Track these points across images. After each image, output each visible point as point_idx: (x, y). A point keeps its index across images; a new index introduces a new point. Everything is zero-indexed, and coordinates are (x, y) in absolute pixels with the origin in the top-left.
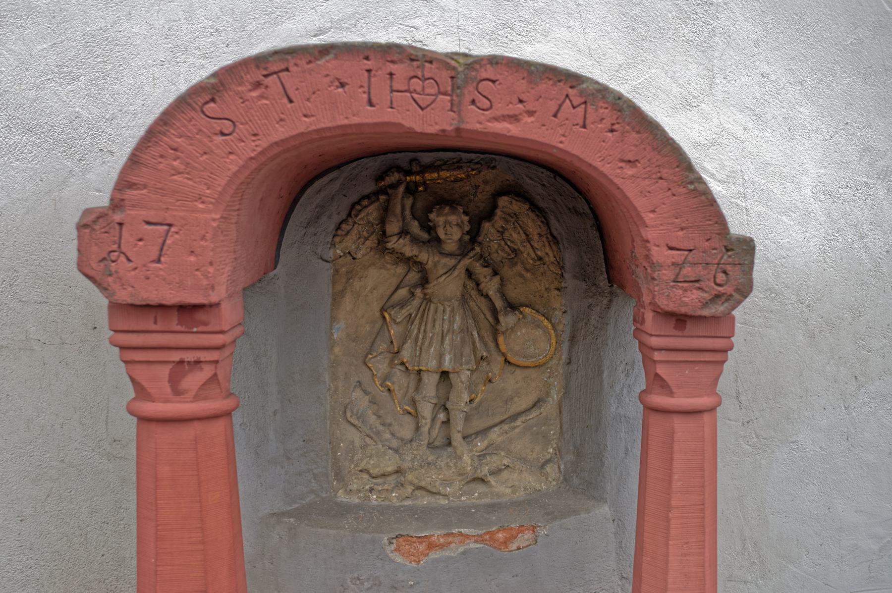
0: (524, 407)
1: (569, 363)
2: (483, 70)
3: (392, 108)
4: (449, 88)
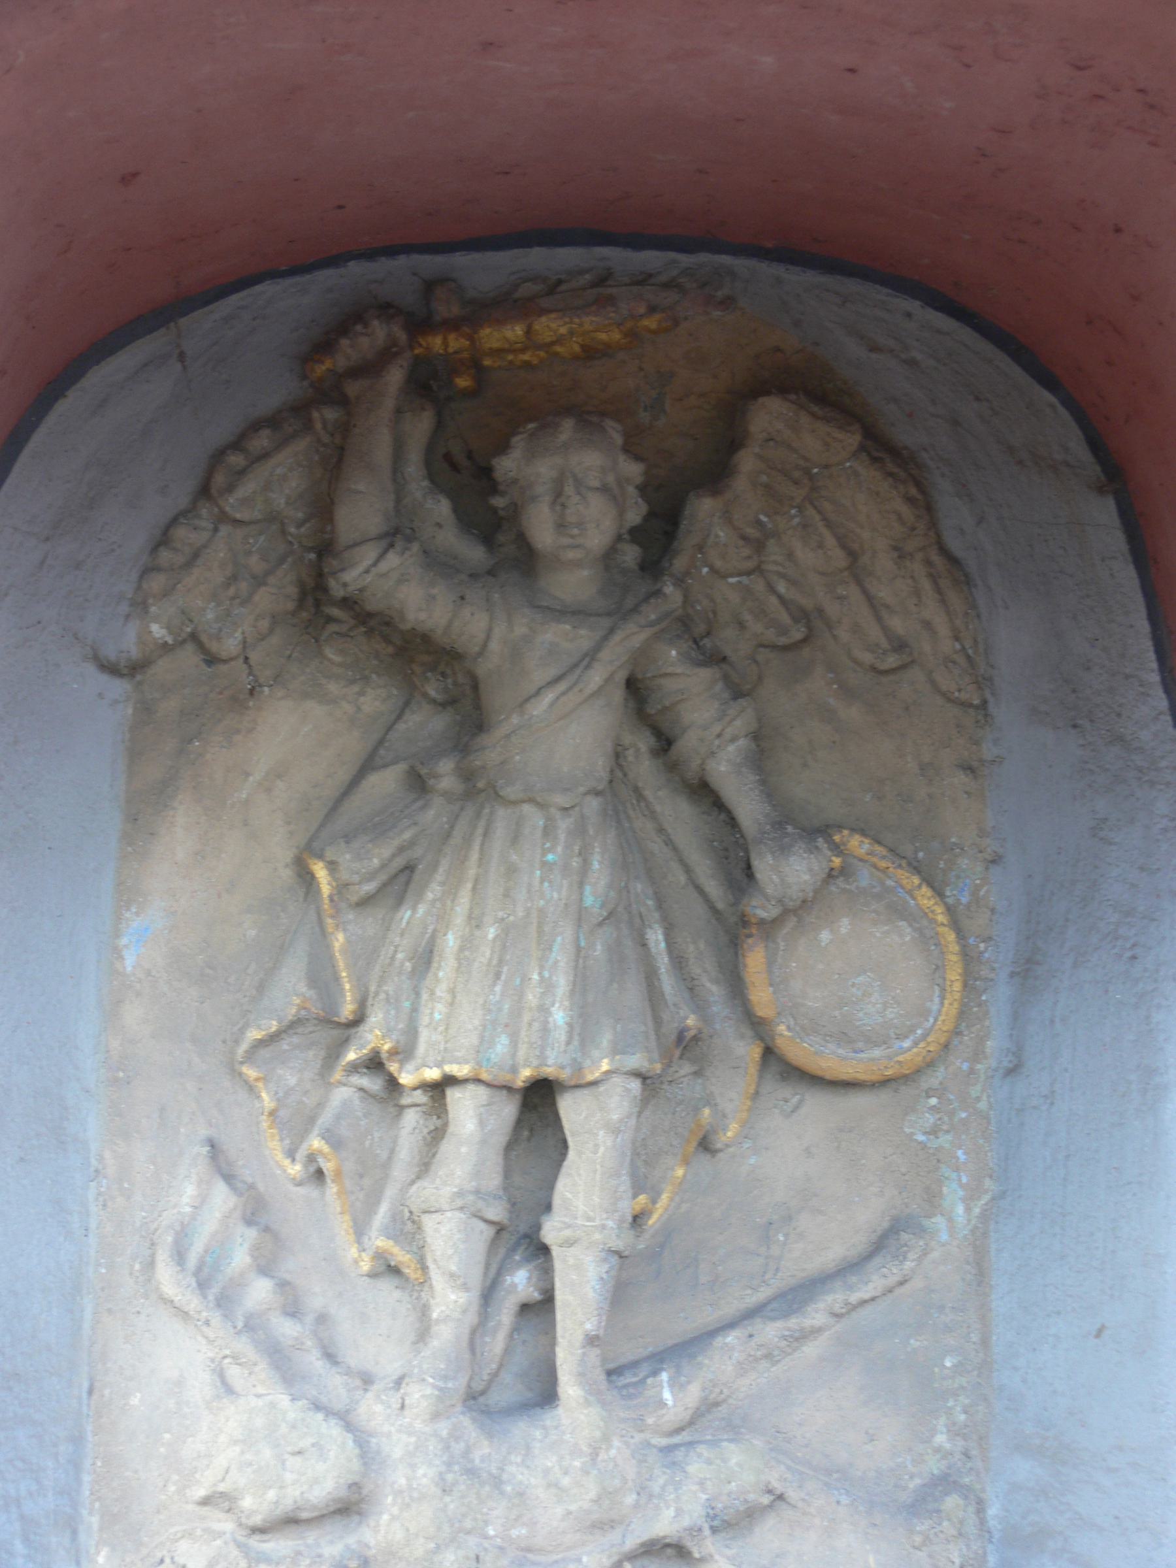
1: (1012, 1071)
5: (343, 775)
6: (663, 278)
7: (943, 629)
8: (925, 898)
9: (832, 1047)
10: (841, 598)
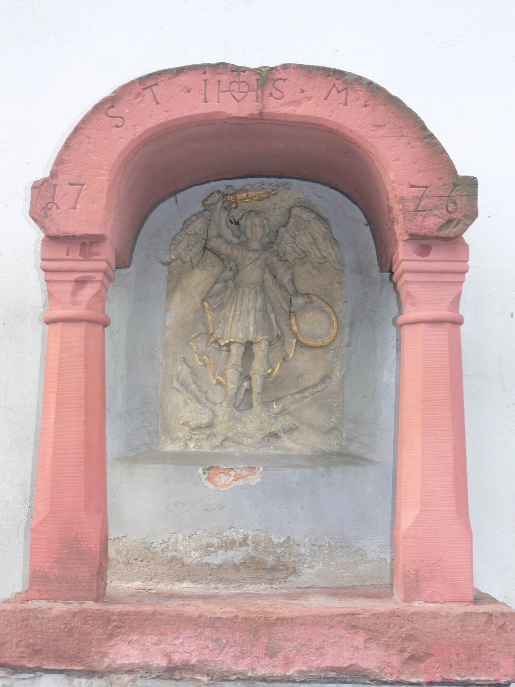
0: (312, 383)
2: (278, 73)
3: (219, 102)
4: (256, 87)
5: (210, 285)
7: (333, 254)
10: (312, 248)
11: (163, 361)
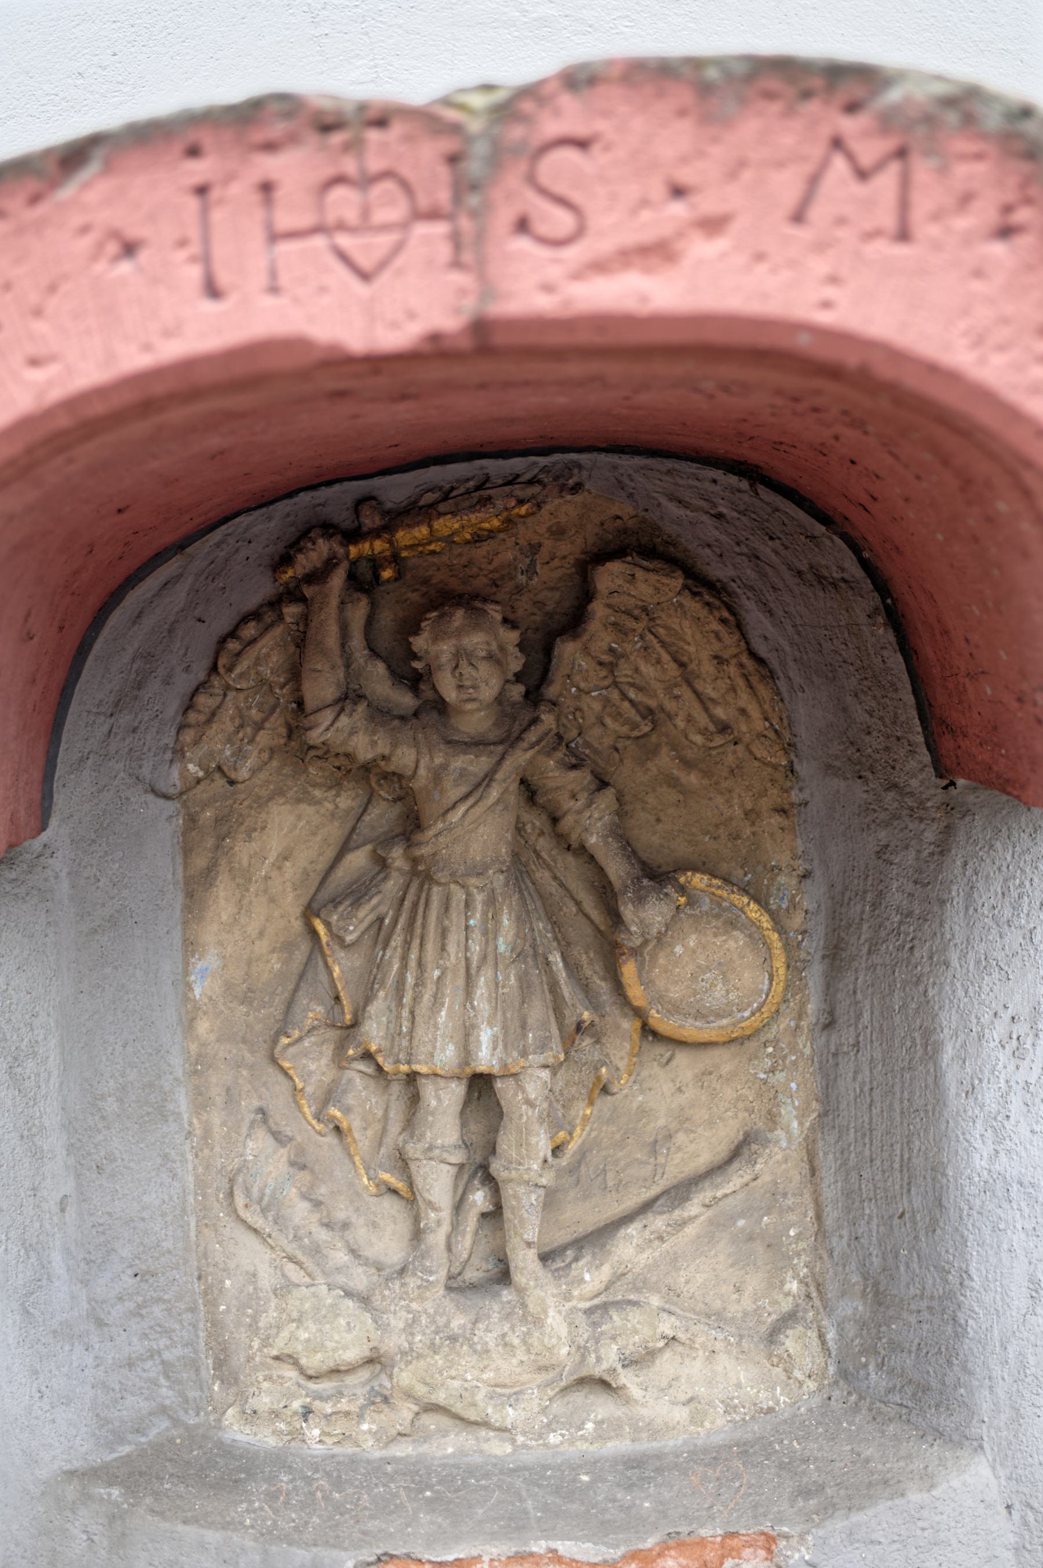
6: (527, 477)
7: (755, 712)
8: (754, 911)
9: (690, 1021)
11: (195, 1121)
